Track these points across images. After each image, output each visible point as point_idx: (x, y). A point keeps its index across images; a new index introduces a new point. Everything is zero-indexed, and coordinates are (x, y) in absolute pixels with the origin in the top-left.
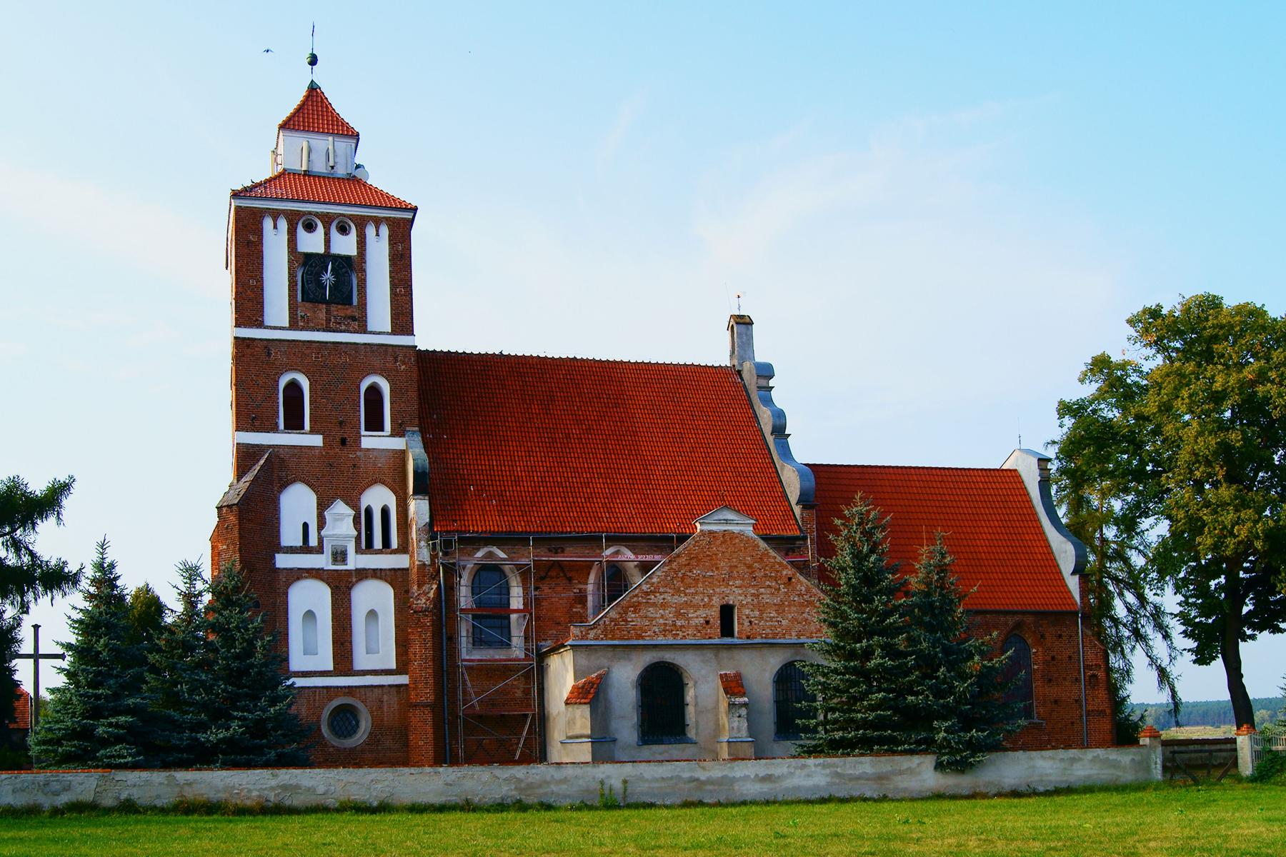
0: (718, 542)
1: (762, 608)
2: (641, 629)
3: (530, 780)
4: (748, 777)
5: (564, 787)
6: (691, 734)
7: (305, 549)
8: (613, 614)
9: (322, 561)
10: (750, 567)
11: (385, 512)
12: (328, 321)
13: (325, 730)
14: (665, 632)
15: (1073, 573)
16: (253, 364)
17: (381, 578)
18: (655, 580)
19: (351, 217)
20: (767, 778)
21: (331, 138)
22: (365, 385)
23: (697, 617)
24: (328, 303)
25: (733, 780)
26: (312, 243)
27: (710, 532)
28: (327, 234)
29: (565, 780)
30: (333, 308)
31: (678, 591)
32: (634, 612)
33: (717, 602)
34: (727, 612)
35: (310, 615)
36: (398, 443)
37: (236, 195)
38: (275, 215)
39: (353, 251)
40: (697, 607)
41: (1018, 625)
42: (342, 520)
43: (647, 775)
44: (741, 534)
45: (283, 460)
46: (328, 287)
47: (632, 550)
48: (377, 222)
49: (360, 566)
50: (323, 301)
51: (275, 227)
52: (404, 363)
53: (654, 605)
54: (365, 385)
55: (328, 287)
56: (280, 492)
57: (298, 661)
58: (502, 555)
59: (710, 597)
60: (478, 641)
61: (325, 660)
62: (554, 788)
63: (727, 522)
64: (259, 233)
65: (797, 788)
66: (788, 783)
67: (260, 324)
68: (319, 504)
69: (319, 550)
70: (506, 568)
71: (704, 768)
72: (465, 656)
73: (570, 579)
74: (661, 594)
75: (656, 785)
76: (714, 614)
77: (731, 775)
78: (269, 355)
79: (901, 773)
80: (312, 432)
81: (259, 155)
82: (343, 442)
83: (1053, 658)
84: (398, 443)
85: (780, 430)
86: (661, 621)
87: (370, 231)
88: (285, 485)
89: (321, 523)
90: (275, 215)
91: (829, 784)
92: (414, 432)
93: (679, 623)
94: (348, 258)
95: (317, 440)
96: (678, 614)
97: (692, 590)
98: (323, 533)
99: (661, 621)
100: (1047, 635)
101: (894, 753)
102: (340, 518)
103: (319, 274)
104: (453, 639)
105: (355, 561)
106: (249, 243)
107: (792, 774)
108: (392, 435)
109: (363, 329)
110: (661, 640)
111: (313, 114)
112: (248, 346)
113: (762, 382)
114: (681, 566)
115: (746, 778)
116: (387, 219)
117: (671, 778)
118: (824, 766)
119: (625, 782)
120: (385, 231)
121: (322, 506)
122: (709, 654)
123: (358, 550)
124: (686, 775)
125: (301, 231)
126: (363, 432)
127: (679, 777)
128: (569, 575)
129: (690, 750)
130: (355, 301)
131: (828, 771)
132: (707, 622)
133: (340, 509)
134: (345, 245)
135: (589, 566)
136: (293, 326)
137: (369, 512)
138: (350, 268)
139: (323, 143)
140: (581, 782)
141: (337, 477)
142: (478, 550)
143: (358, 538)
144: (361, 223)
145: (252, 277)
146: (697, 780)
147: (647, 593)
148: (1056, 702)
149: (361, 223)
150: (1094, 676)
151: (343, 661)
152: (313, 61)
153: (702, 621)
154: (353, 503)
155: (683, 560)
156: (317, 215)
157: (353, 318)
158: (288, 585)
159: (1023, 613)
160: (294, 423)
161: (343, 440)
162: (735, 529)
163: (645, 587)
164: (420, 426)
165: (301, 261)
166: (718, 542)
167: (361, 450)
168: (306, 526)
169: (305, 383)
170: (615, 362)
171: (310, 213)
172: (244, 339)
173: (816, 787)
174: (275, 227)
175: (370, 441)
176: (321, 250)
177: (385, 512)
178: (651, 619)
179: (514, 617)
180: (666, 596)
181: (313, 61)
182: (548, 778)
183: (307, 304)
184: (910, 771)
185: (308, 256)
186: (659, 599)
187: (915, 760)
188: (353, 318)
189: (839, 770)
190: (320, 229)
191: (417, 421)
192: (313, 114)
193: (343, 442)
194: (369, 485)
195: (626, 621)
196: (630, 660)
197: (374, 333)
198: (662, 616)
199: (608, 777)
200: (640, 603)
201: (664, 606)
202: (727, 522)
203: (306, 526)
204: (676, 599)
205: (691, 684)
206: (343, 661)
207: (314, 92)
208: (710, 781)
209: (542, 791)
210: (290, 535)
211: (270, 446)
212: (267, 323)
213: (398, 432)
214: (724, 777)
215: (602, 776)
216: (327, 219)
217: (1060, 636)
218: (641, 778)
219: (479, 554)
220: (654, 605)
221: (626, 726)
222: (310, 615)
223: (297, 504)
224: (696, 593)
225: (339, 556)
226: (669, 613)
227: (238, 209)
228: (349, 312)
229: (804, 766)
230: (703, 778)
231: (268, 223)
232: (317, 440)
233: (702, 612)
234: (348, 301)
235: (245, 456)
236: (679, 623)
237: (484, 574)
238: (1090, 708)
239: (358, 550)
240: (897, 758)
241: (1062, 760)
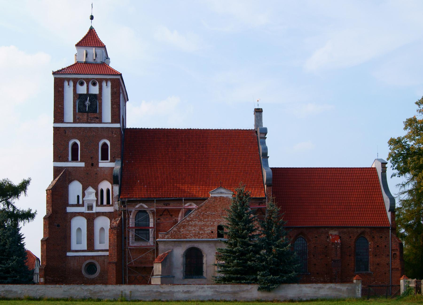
0: (218, 201)
2: (186, 235)
3: (95, 290)
4: (180, 291)
5: (108, 293)
6: (205, 275)
7: (78, 205)
8: (175, 229)
9: (83, 210)
12: (88, 119)
13: (83, 272)
14: (195, 236)
15: (389, 211)
16: (60, 136)
17: (105, 216)
18: (192, 216)
19: (97, 79)
20: (188, 292)
21: (94, 49)
22: (101, 143)
23: (208, 230)
24: (88, 112)
25: (174, 292)
26: (82, 90)
27: (215, 197)
29: (108, 291)
30: (89, 114)
31: (201, 220)
32: (183, 228)
33: (216, 224)
35: (79, 230)
36: (112, 165)
37: (54, 73)
38: (69, 80)
40: (208, 226)
41: (363, 233)
42: (91, 194)
43: (140, 290)
44: (227, 198)
45: (70, 172)
46: (88, 106)
47: (196, 204)
48: (107, 80)
49: (97, 211)
50: (85, 112)
51: (69, 85)
52: (115, 134)
53: (191, 225)
54: (101, 143)
55: (88, 106)
57: (74, 246)
58: (146, 207)
59: (213, 222)
60: (137, 239)
61: (84, 246)
62: (104, 293)
63: (221, 193)
64: (63, 87)
65: (199, 296)
66: (196, 294)
67: (62, 122)
68: (83, 188)
69: (83, 205)
70: (148, 211)
71: (162, 288)
72: (131, 244)
73: (172, 215)
74: (194, 221)
75: (143, 293)
76: (215, 229)
77: (173, 290)
78: (65, 133)
79: (243, 291)
80: (81, 161)
81: (68, 57)
82: (92, 165)
83: (378, 246)
84: (112, 165)
85: (265, 156)
86: (194, 232)
87: (104, 84)
88: (70, 181)
89: (84, 195)
90: (69, 80)
91: (213, 295)
92: (118, 160)
93: (201, 232)
94: (95, 95)
95: (82, 164)
96: (200, 229)
97: (207, 220)
98: (84, 199)
99: (194, 232)
100: (375, 237)
101: (241, 283)
102: (90, 193)
103: (84, 102)
104: (126, 238)
105: (96, 209)
106: (59, 91)
107: (197, 290)
108: (111, 162)
109: (101, 122)
110: (193, 239)
111: (91, 39)
112: (58, 130)
113: (262, 136)
114: (202, 210)
115: (179, 292)
116: (111, 80)
117: (149, 291)
118: (211, 288)
119: (131, 292)
120: (109, 84)
122: (212, 244)
123: (97, 205)
124: (155, 290)
125: (78, 86)
126: (100, 161)
127: (152, 291)
128: (171, 214)
129: (204, 281)
130: (98, 112)
131: (212, 290)
132: (212, 232)
133: (91, 190)
134: (94, 90)
135: (179, 210)
136: (75, 122)
137: (102, 191)
138: (96, 99)
139: (92, 51)
140: (114, 292)
141: (90, 178)
142: (137, 205)
143: (97, 201)
144: (101, 81)
145: (60, 104)
146: (160, 292)
147: (189, 221)
148: (378, 264)
149: (101, 81)
150: (395, 254)
151: (91, 246)
152: (92, 18)
153: (210, 231)
154: (96, 188)
155: (203, 208)
156: (84, 79)
157: (97, 118)
158: (71, 218)
159: (365, 228)
160: (75, 158)
161: (92, 163)
162: (224, 196)
164: (121, 158)
165: (78, 97)
166: (218, 201)
167: (99, 168)
168: (78, 197)
170: (206, 130)
171: (81, 78)
172: (57, 128)
173: (207, 296)
175: (103, 164)
176: (85, 92)
177: (108, 191)
178: (190, 231)
179: (150, 230)
180: (196, 222)
181: (92, 18)
182: (102, 290)
183: (80, 113)
184: (247, 291)
185: (81, 95)
186: (193, 223)
187: (250, 286)
188: (97, 118)
189: (217, 289)
190: (85, 84)
191: (120, 156)
192: (91, 39)
193: (92, 165)
195: (180, 232)
196: (181, 246)
198: (194, 230)
199: (125, 290)
200: (185, 225)
201: (195, 226)
202: (221, 193)
203: (78, 197)
204: (200, 223)
205: (205, 256)
206: (91, 246)
207: (92, 31)
208: (164, 292)
209: (99, 294)
210: (72, 200)
211: (65, 167)
213: (112, 161)
214: (170, 291)
215: (122, 290)
216: (88, 80)
217: (381, 237)
218: (138, 291)
219: (137, 206)
220: (191, 225)
221: (179, 271)
222: (79, 230)
223: (75, 188)
224: (208, 221)
225: (90, 207)
226: (197, 229)
227: (55, 79)
228: (95, 115)
229: (203, 288)
230: (162, 291)
231: (66, 83)
232: (82, 164)
233: (210, 228)
234: (95, 111)
235: (57, 171)
236: (201, 232)
237: (140, 214)
238: (393, 267)
239: (97, 205)
240: (242, 285)
241: (315, 288)
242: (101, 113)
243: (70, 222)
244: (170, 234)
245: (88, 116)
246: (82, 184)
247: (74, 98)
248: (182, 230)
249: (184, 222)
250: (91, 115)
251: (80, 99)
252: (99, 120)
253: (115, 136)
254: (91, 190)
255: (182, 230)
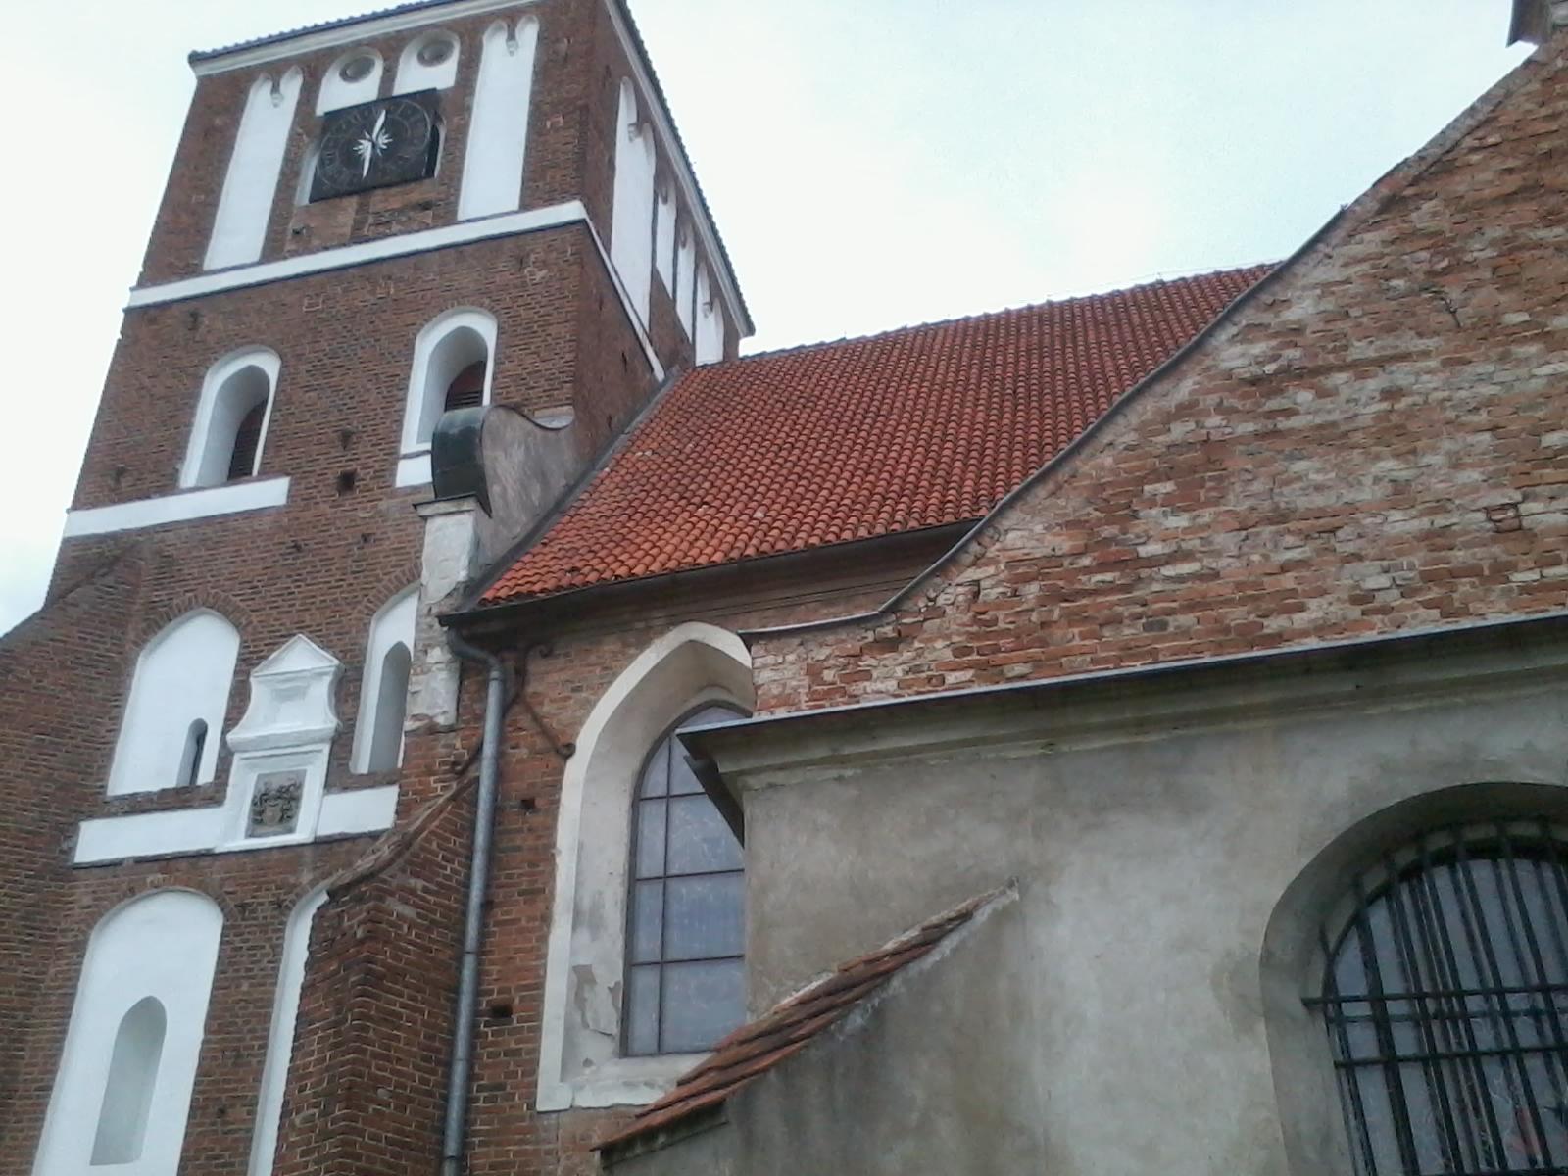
2: (1251, 593)
7: (182, 798)
16: (159, 352)
31: (1489, 331)
35: (146, 1021)
49: (328, 829)
53: (1329, 438)
74: (1360, 369)
80: (266, 474)
82: (347, 482)
86: (1401, 523)
98: (230, 737)
99: (1401, 523)
102: (291, 690)
158: (96, 914)
167: (395, 493)
168: (199, 733)
171: (358, 44)
172: (146, 308)
178: (1325, 526)
180: (1401, 375)
186: (1358, 398)
193: (347, 482)
195: (1130, 563)
198: (1400, 494)
200: (1212, 449)
203: (199, 733)
204: (1485, 378)
210: (144, 756)
225: (277, 803)
232: (272, 493)
243: (80, 948)
244: (957, 621)
248: (1160, 527)
249: (1186, 410)
253: (540, 275)
255: (1160, 527)
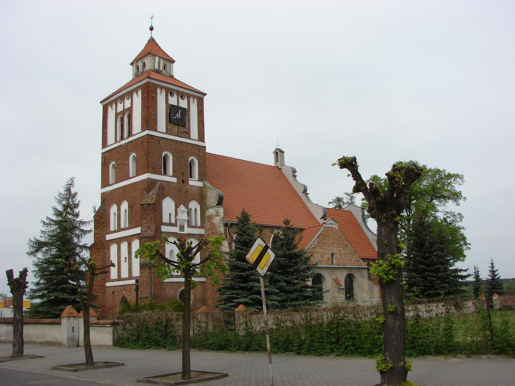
1: (340, 254)
7: (170, 224)
10: (337, 240)
11: (196, 210)
12: (178, 132)
19: (186, 94)
24: (178, 125)
26: (173, 101)
27: (328, 227)
28: (178, 98)
30: (180, 127)
31: (321, 248)
33: (330, 252)
34: (332, 254)
39: (186, 107)
40: (326, 254)
46: (178, 118)
48: (194, 97)
51: (161, 92)
56: (163, 200)
63: (332, 224)
69: (175, 225)
76: (330, 256)
78: (159, 143)
80: (173, 176)
82: (183, 181)
84: (200, 184)
88: (164, 197)
89: (176, 214)
90: (162, 88)
94: (185, 109)
95: (174, 180)
96: (322, 256)
97: (324, 248)
102: (183, 212)
105: (187, 230)
108: (198, 181)
116: (197, 96)
121: (177, 207)
125: (169, 95)
133: (182, 208)
134: (183, 104)
136: (167, 133)
138: (185, 112)
141: (182, 197)
152: (152, 29)
154: (187, 206)
155: (321, 237)
157: (186, 133)
162: (334, 226)
163: (313, 246)
167: (189, 185)
168: (170, 214)
169: (171, 157)
171: (173, 89)
174: (161, 92)
176: (176, 104)
177: (196, 210)
181: (152, 29)
183: (172, 125)
186: (316, 250)
188: (186, 133)
190: (175, 97)
192: (152, 49)
193: (183, 181)
194: (191, 200)
197: (192, 139)
201: (318, 253)
202: (332, 224)
203: (170, 214)
211: (159, 181)
212: (158, 130)
224: (325, 249)
225: (182, 228)
228: (185, 130)
231: (159, 91)
232: (174, 180)
233: (327, 256)
234: (184, 126)
239: (189, 226)
242: (189, 129)
245: (178, 129)
246: (175, 201)
247: (166, 107)
250: (182, 129)
251: (172, 110)
252: (187, 134)
254: (182, 208)
